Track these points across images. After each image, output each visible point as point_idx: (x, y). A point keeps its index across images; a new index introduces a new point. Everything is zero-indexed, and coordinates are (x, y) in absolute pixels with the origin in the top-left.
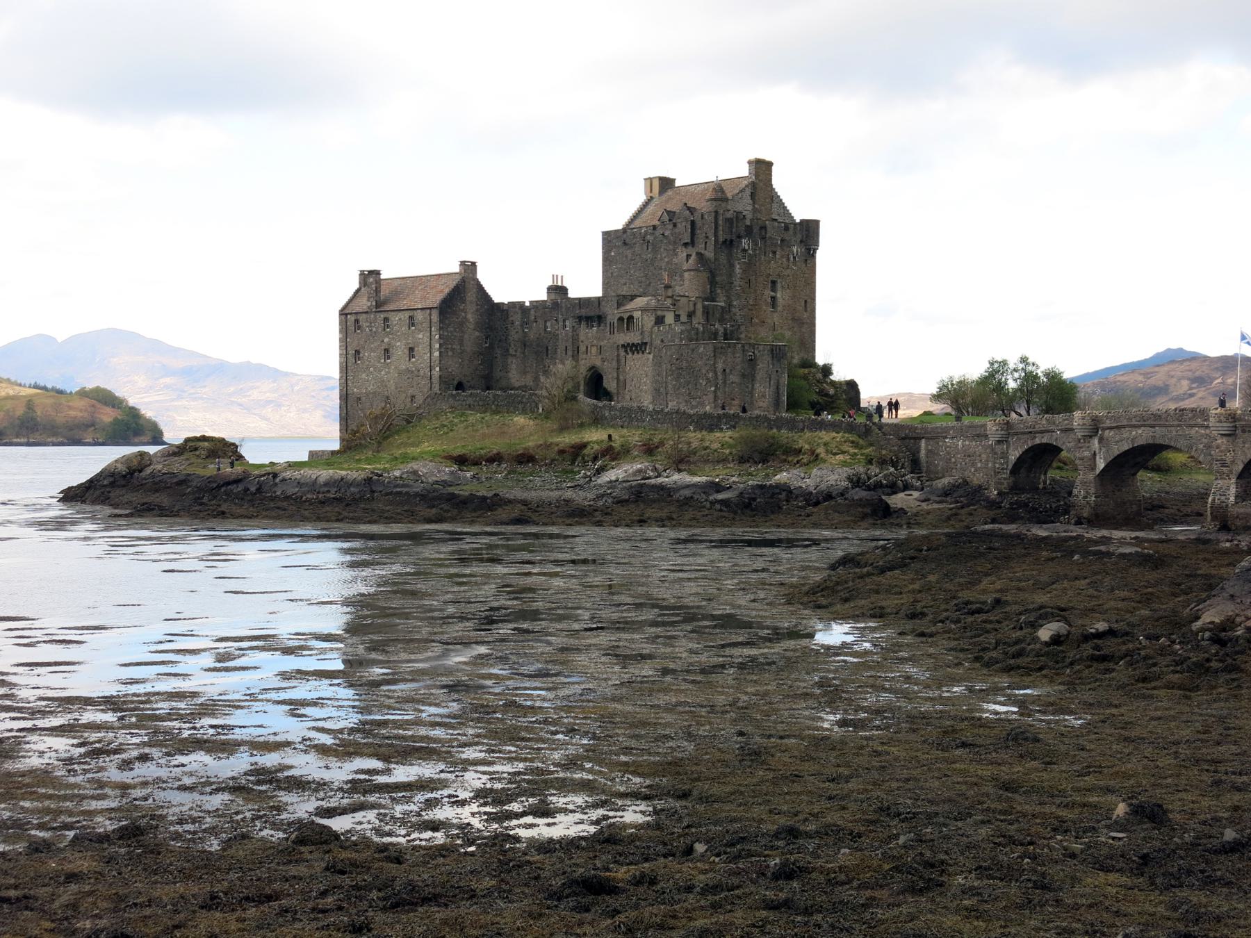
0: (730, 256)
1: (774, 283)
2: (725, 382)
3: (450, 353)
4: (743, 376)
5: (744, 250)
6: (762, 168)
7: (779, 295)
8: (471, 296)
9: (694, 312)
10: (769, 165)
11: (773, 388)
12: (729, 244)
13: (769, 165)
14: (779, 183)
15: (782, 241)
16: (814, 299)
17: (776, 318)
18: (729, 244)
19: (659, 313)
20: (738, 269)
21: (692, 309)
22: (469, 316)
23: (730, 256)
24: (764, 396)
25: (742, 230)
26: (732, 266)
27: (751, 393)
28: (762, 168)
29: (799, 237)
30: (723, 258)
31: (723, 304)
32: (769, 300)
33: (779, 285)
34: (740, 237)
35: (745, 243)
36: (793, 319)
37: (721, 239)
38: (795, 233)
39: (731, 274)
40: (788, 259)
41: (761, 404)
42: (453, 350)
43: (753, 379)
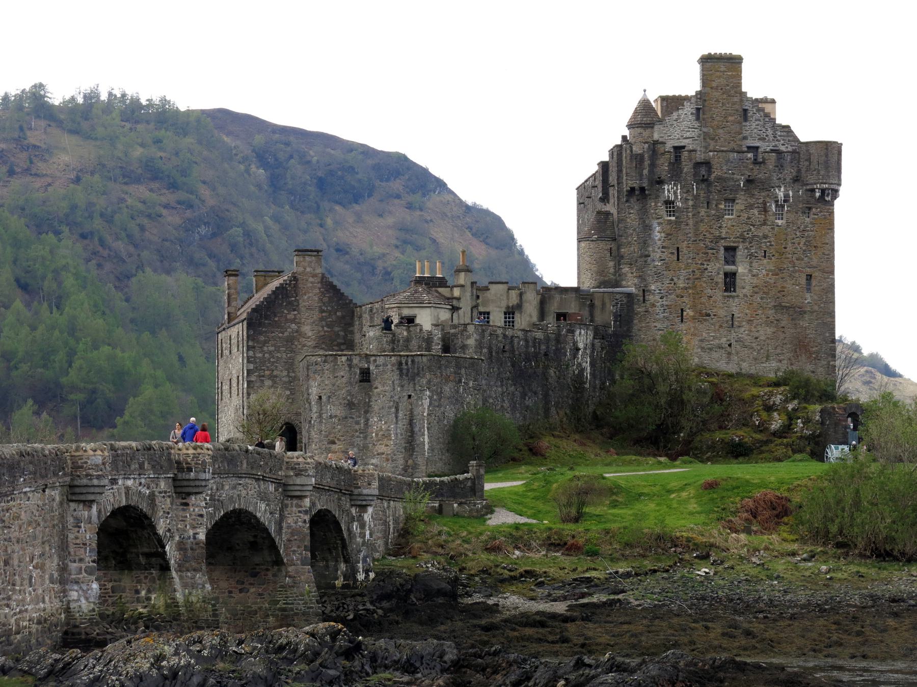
0: (643, 212)
1: (731, 250)
2: (320, 416)
3: (268, 383)
4: (350, 405)
5: (668, 203)
6: (721, 69)
7: (741, 269)
8: (310, 297)
9: (519, 306)
10: (733, 63)
11: (403, 424)
12: (639, 194)
13: (733, 63)
14: (753, 85)
15: (749, 181)
16: (829, 271)
17: (736, 306)
18: (639, 194)
19: (406, 312)
20: (657, 234)
21: (514, 299)
22: (307, 329)
23: (643, 212)
24: (388, 437)
25: (663, 167)
26: (647, 228)
27: (365, 432)
28: (721, 69)
29: (789, 172)
30: (632, 219)
31: (633, 290)
32: (720, 278)
33: (741, 254)
34: (661, 182)
35: (669, 191)
36: (779, 307)
37: (626, 188)
38: (780, 166)
39: (645, 243)
40: (765, 210)
41: (382, 448)
42: (272, 377)
43: (367, 409)
